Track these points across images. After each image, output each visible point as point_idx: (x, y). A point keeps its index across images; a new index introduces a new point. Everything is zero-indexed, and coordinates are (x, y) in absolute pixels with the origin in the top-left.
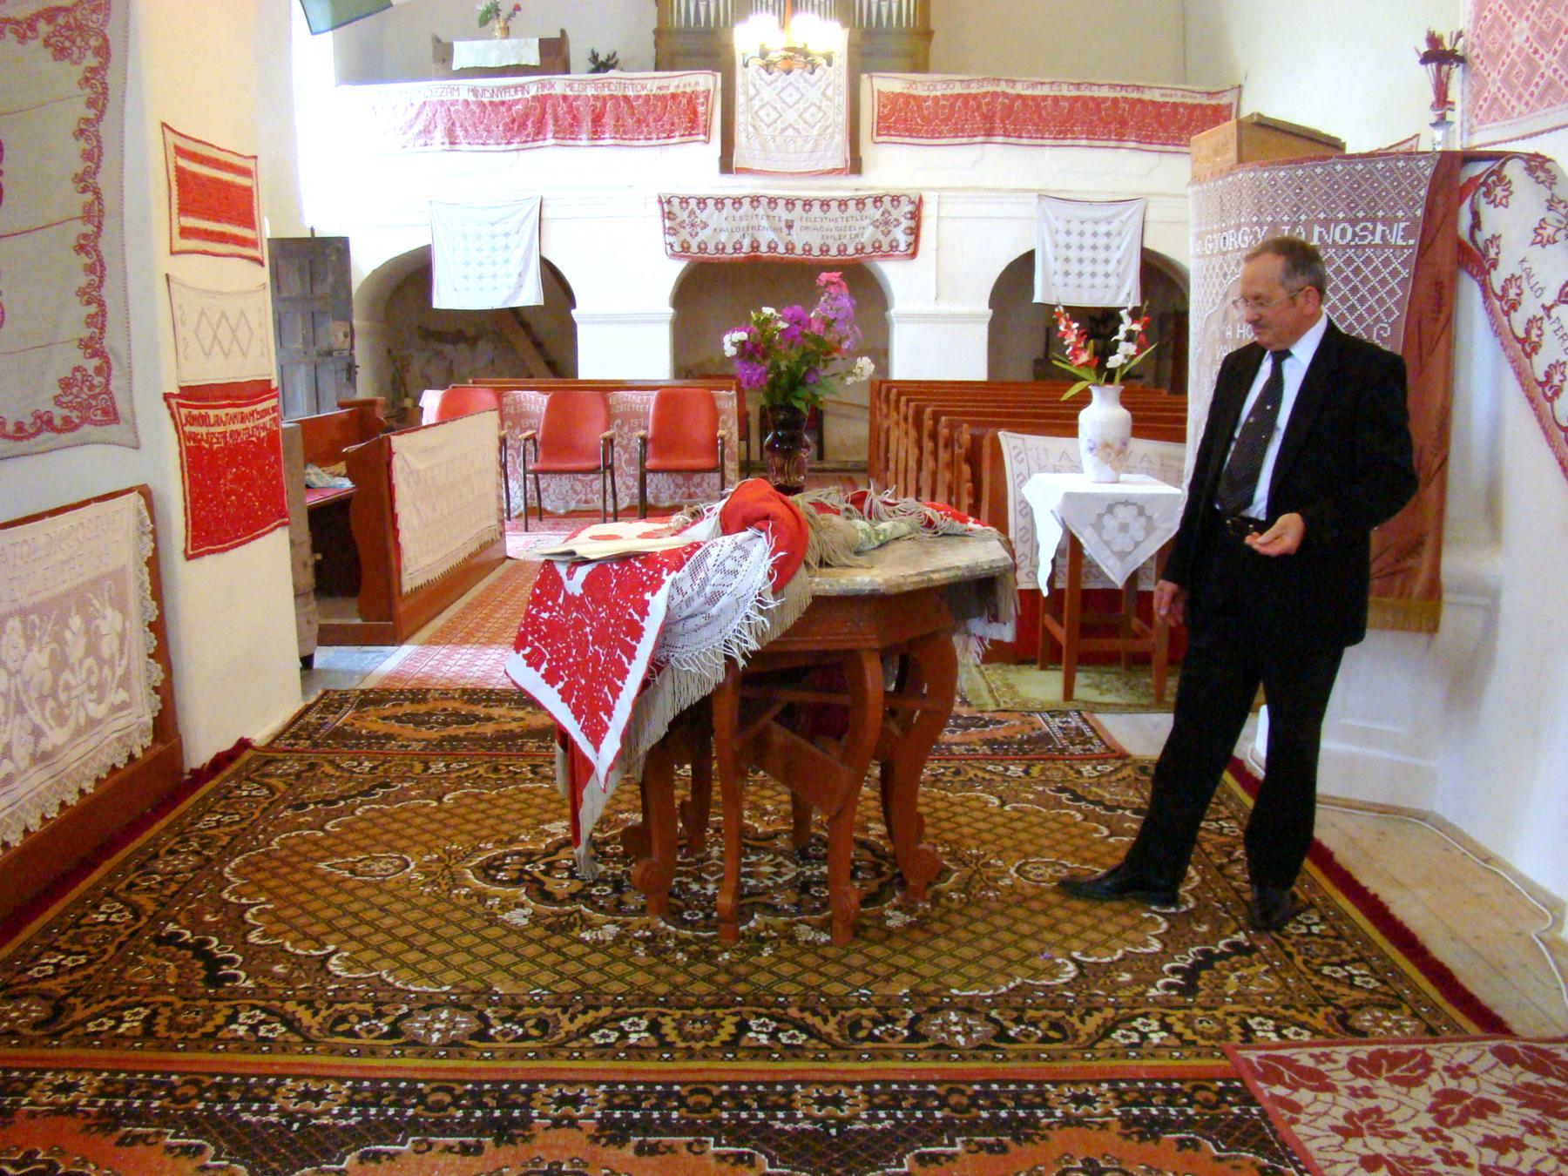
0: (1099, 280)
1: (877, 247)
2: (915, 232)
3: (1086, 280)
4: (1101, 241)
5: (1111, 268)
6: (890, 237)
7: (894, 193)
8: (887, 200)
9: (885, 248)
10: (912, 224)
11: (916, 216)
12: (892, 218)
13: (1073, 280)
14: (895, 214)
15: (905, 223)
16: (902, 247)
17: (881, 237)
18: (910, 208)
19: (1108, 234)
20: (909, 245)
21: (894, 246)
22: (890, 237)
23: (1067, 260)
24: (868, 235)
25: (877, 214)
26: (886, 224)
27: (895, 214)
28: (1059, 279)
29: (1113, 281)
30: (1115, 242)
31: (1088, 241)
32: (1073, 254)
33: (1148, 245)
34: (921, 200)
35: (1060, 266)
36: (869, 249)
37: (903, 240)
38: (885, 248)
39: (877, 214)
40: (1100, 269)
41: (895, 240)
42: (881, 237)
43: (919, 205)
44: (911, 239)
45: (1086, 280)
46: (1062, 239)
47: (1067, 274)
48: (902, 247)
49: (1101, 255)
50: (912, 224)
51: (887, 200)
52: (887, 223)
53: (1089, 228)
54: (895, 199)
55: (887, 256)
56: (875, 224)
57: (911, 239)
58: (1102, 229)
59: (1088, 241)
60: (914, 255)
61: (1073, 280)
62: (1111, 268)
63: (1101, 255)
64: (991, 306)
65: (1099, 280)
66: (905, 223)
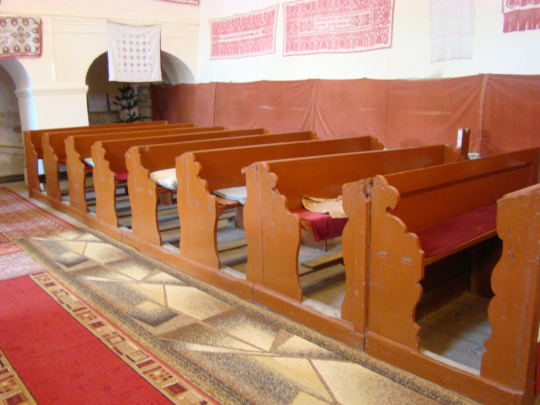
0: (142, 68)
1: (17, 50)
2: (39, 40)
3: (135, 68)
4: (141, 47)
5: (147, 61)
6: (25, 44)
7: (23, 16)
8: (20, 21)
9: (22, 50)
10: (38, 36)
11: (39, 31)
12: (24, 32)
13: (129, 68)
14: (26, 29)
15: (33, 35)
16: (33, 50)
17: (19, 44)
18: (35, 26)
19: (144, 43)
20: (37, 49)
21: (28, 49)
22: (25, 44)
23: (125, 57)
24: (11, 42)
25: (15, 29)
26: (21, 35)
27: (26, 29)
28: (122, 67)
29: (148, 68)
30: (147, 47)
31: (135, 47)
32: (128, 54)
33: (162, 49)
34: (41, 22)
35: (122, 61)
36: (12, 51)
37: (33, 46)
38: (22, 50)
39: (15, 29)
40: (142, 62)
41: (28, 45)
42: (19, 44)
43: (40, 24)
44: (38, 45)
45: (135, 68)
46: (121, 45)
47: (125, 64)
48: (33, 50)
49: (141, 54)
50: (38, 36)
51: (20, 21)
52: (21, 35)
53: (134, 40)
54: (25, 21)
55: (23, 56)
56: (14, 35)
57: (38, 45)
58: (141, 40)
59: (135, 47)
60: (40, 55)
61: (129, 68)
62: (147, 61)
63: (141, 54)
64: (87, 84)
65: (142, 68)
66: (33, 35)
